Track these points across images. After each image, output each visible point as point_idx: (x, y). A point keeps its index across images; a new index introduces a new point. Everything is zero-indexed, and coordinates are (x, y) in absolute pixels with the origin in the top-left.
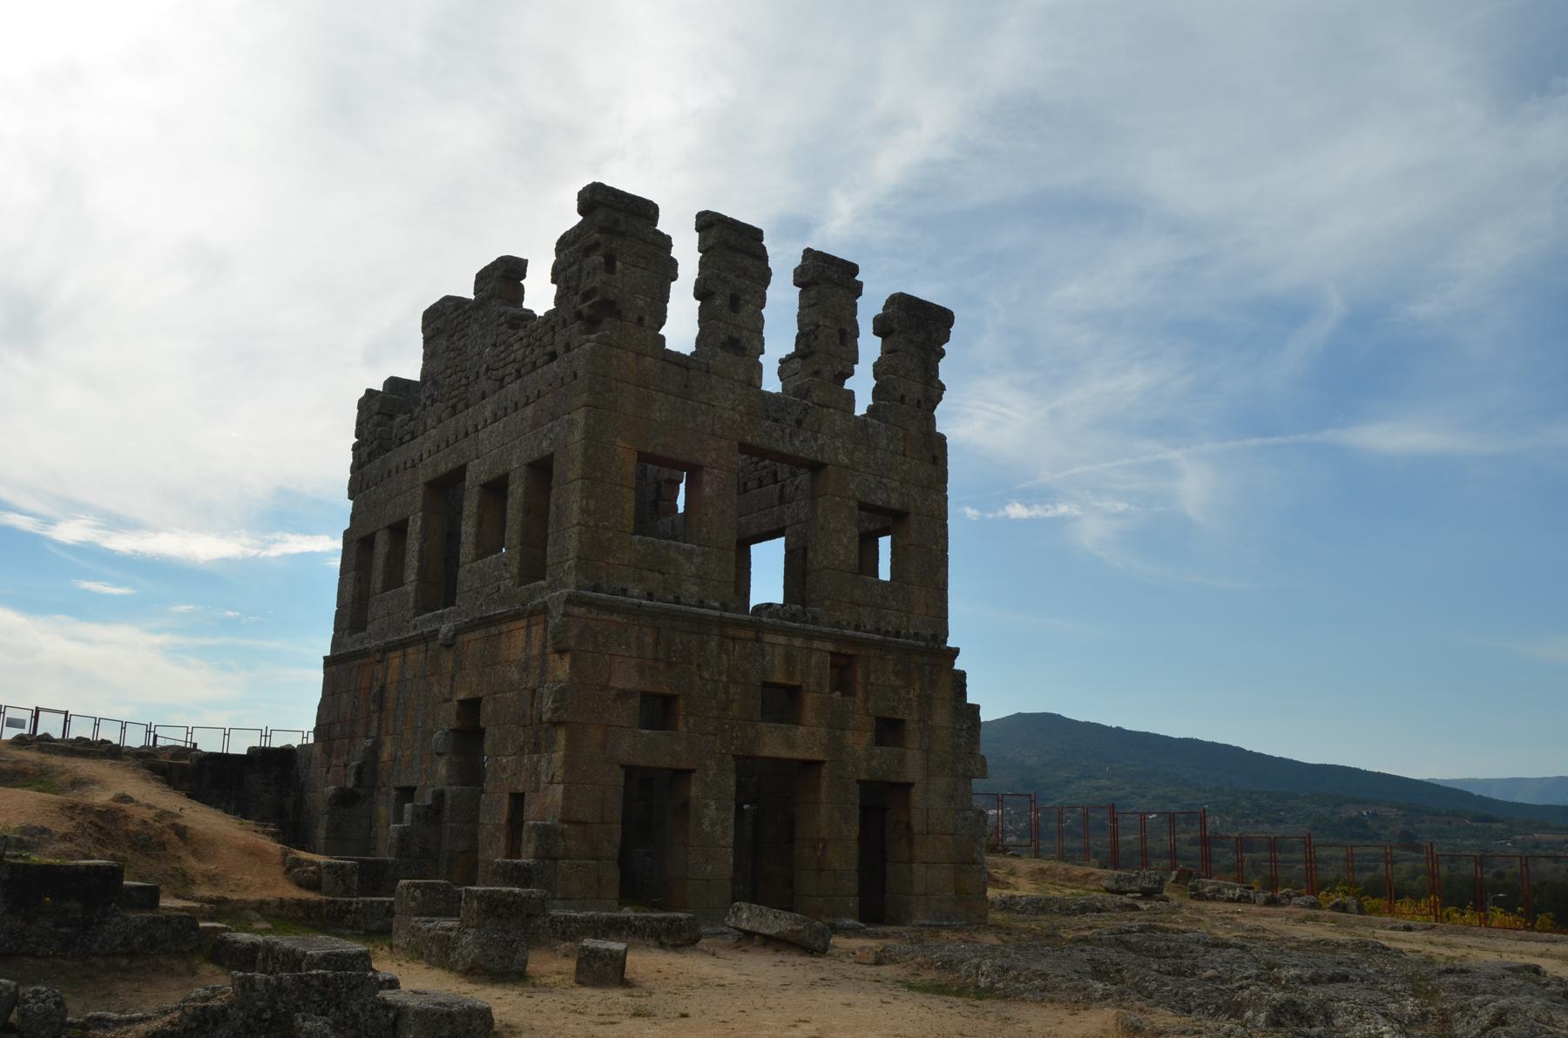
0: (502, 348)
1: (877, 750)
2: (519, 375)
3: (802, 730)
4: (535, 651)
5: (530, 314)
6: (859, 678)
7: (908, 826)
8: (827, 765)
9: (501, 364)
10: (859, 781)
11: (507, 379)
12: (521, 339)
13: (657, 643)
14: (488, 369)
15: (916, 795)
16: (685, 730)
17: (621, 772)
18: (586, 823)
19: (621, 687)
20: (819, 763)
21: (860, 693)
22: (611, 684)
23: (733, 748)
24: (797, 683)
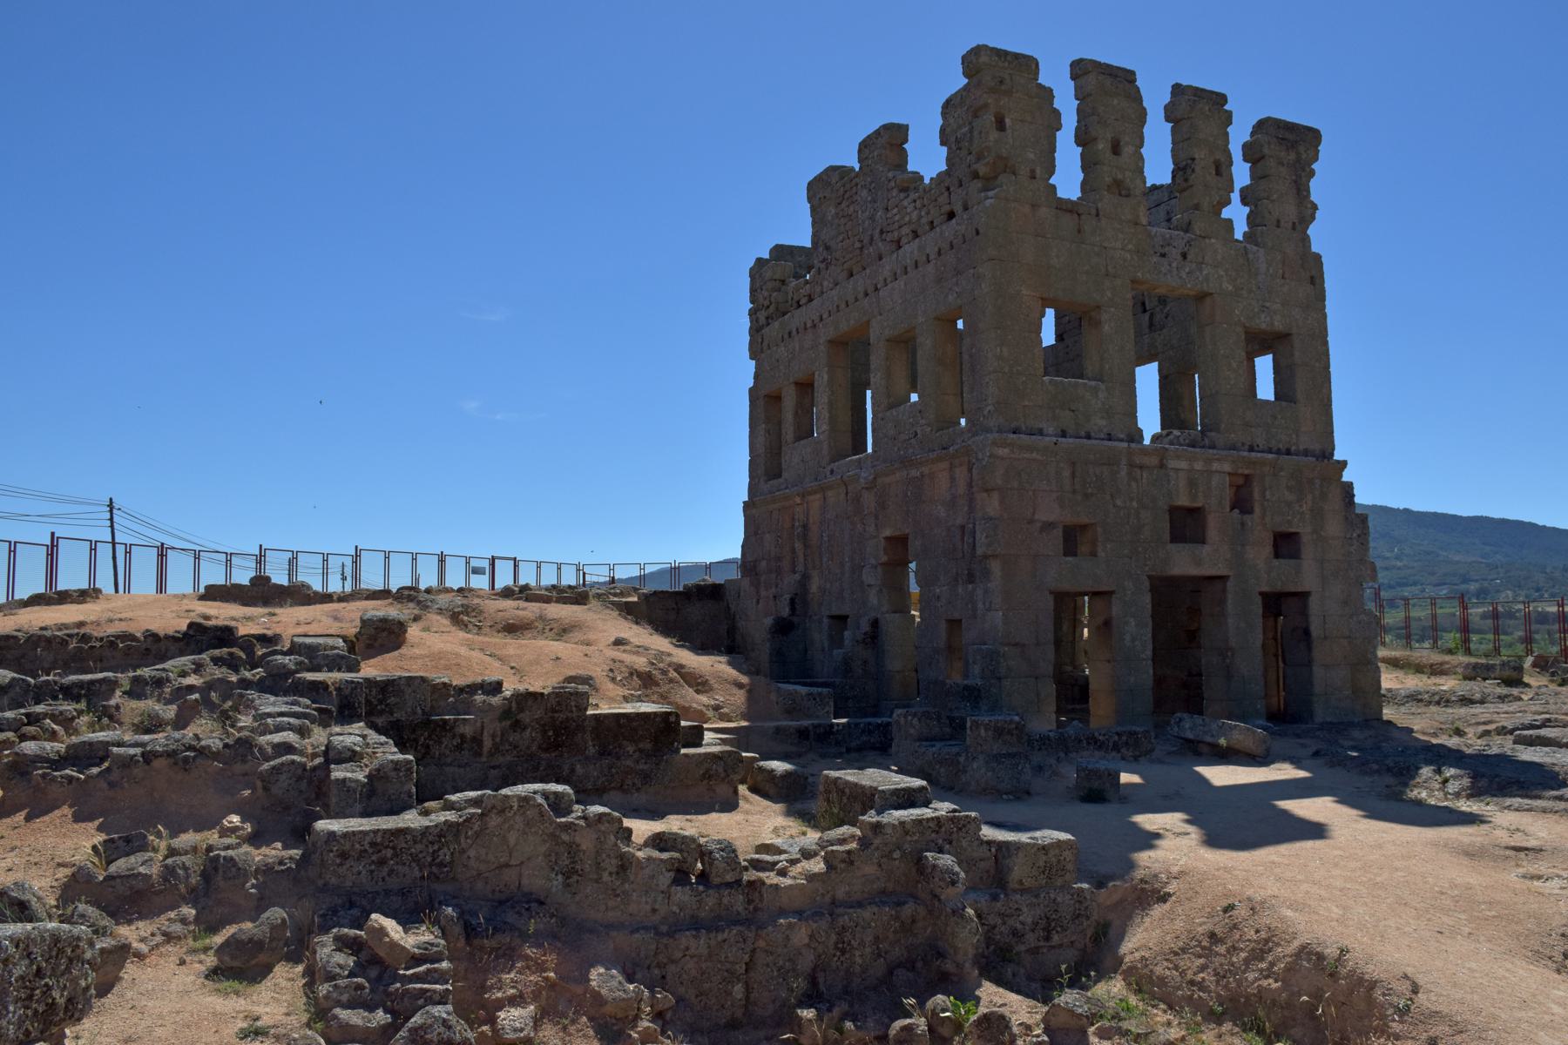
0: (895, 210)
1: (1276, 562)
2: (916, 235)
3: (1207, 549)
4: (962, 489)
5: (918, 177)
6: (1256, 495)
7: (1307, 632)
8: (1231, 579)
9: (896, 225)
10: (1261, 594)
11: (904, 240)
12: (915, 201)
13: (1073, 475)
14: (882, 232)
15: (1314, 604)
16: (1103, 554)
17: (1051, 599)
18: (1024, 645)
19: (1045, 519)
20: (1223, 579)
21: (1257, 510)
22: (1036, 517)
23: (1147, 568)
24: (1200, 505)
